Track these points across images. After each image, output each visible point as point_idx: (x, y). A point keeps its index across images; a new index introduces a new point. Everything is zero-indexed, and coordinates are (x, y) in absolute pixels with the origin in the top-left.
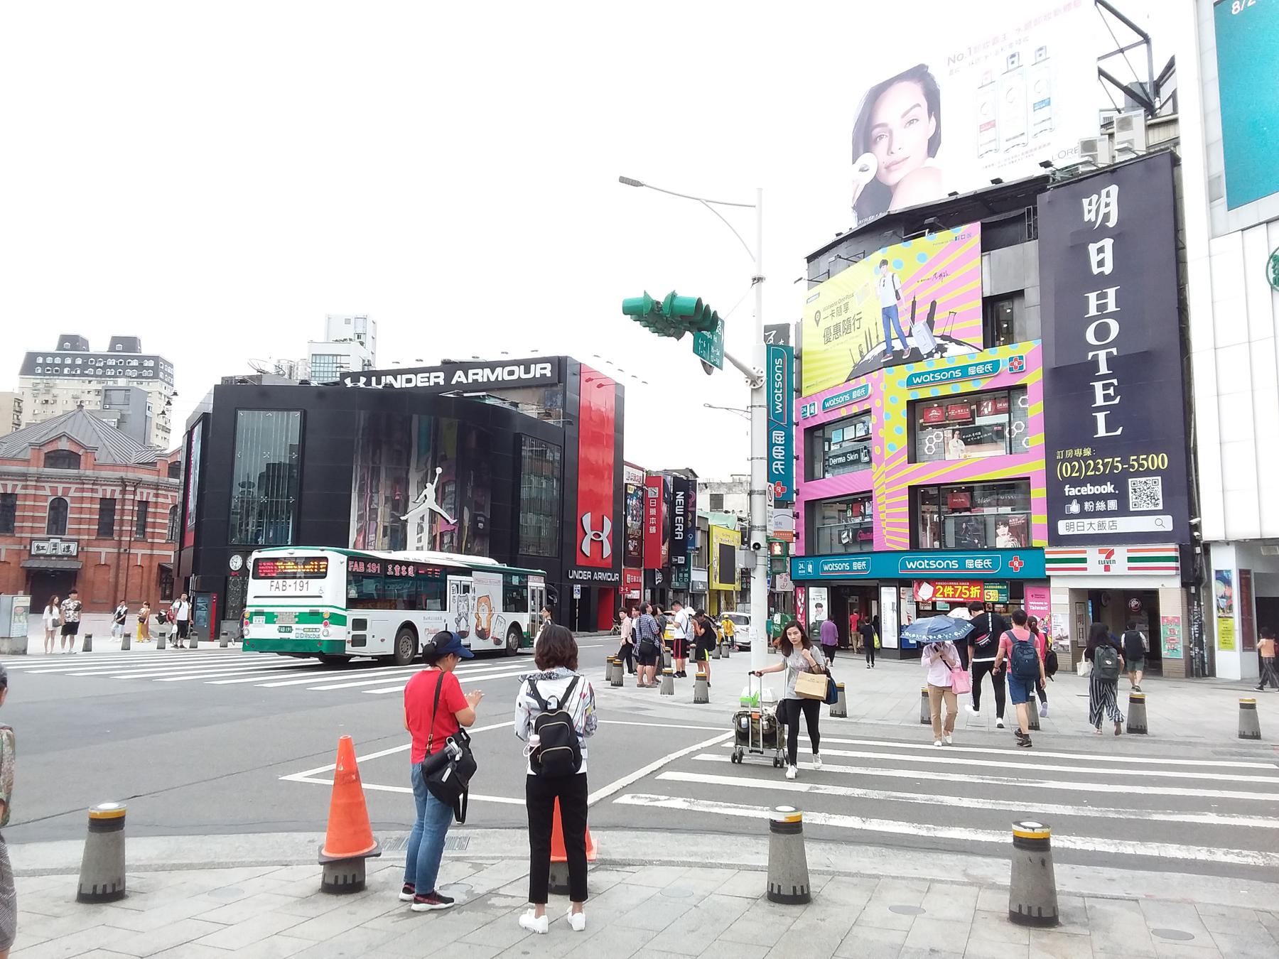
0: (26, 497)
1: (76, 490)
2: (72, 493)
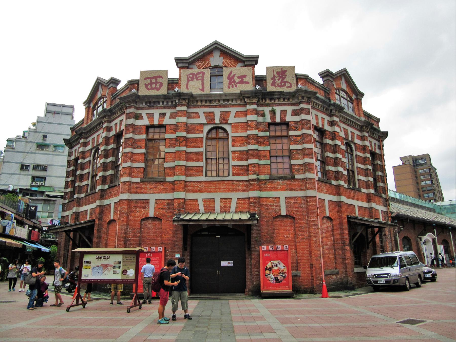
0: (175, 128)
1: (237, 114)
2: (232, 119)
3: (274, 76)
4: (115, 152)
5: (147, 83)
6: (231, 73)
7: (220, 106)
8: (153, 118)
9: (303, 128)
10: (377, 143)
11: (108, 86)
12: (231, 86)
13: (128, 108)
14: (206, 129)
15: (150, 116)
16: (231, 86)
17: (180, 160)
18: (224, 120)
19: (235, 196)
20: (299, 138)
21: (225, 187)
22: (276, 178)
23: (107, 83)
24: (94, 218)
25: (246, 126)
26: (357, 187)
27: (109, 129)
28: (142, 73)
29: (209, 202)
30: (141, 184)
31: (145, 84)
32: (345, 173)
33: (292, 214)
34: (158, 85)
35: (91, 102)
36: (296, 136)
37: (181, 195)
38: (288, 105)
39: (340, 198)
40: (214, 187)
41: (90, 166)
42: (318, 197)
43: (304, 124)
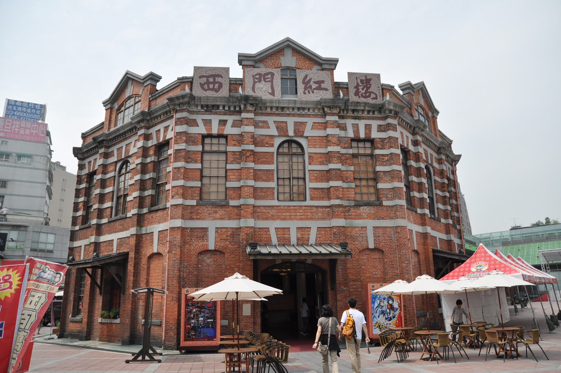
0: (240, 139)
1: (315, 126)
2: (308, 132)
3: (358, 85)
4: (157, 166)
5: (202, 83)
6: (306, 76)
7: (294, 115)
8: (211, 126)
9: (391, 147)
10: (450, 167)
11: (144, 83)
12: (307, 91)
13: (180, 112)
14: (277, 142)
15: (208, 123)
16: (307, 91)
17: (247, 179)
18: (299, 132)
19: (314, 225)
20: (386, 158)
21: (302, 214)
22: (361, 203)
23: (143, 79)
24: (126, 251)
25: (327, 140)
26: (436, 216)
27: (147, 137)
28: (196, 69)
29: (283, 233)
30: (197, 208)
31: (200, 83)
32: (428, 201)
33: (380, 247)
34: (217, 86)
35: (115, 103)
36: (383, 155)
37: (251, 222)
38: (373, 119)
39: (427, 229)
40: (288, 214)
41: (114, 183)
42: (408, 228)
43: (392, 141)
